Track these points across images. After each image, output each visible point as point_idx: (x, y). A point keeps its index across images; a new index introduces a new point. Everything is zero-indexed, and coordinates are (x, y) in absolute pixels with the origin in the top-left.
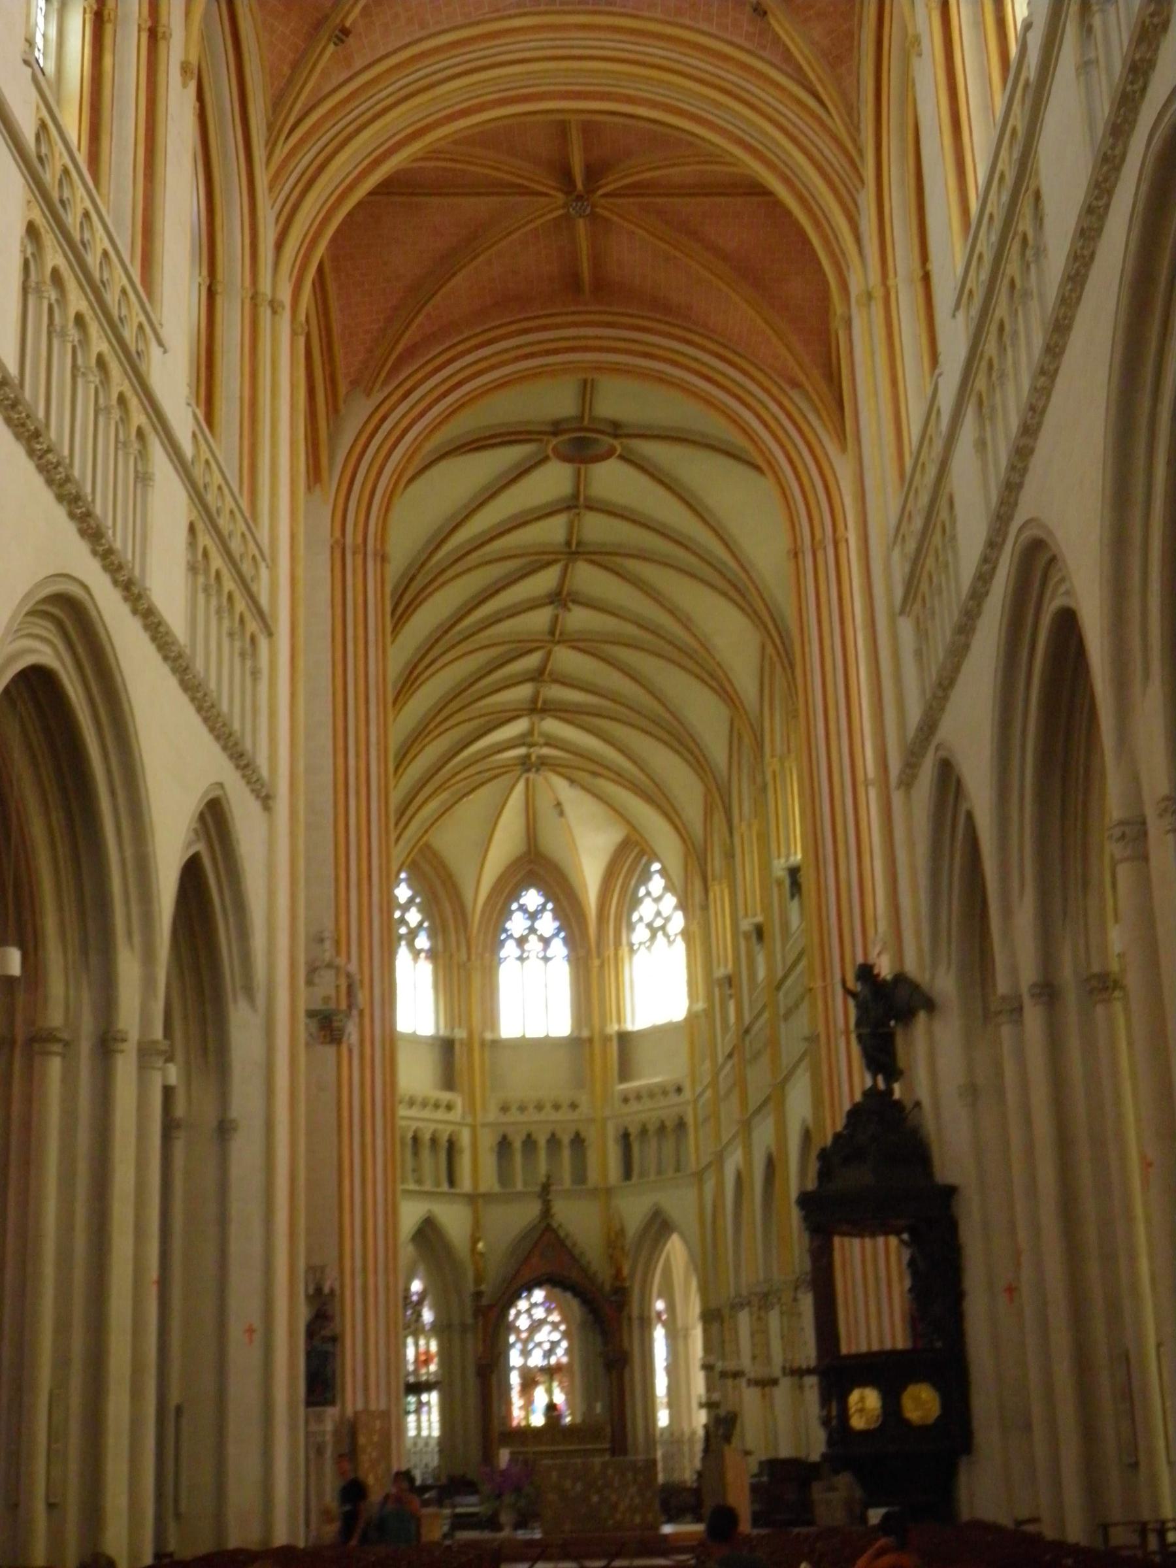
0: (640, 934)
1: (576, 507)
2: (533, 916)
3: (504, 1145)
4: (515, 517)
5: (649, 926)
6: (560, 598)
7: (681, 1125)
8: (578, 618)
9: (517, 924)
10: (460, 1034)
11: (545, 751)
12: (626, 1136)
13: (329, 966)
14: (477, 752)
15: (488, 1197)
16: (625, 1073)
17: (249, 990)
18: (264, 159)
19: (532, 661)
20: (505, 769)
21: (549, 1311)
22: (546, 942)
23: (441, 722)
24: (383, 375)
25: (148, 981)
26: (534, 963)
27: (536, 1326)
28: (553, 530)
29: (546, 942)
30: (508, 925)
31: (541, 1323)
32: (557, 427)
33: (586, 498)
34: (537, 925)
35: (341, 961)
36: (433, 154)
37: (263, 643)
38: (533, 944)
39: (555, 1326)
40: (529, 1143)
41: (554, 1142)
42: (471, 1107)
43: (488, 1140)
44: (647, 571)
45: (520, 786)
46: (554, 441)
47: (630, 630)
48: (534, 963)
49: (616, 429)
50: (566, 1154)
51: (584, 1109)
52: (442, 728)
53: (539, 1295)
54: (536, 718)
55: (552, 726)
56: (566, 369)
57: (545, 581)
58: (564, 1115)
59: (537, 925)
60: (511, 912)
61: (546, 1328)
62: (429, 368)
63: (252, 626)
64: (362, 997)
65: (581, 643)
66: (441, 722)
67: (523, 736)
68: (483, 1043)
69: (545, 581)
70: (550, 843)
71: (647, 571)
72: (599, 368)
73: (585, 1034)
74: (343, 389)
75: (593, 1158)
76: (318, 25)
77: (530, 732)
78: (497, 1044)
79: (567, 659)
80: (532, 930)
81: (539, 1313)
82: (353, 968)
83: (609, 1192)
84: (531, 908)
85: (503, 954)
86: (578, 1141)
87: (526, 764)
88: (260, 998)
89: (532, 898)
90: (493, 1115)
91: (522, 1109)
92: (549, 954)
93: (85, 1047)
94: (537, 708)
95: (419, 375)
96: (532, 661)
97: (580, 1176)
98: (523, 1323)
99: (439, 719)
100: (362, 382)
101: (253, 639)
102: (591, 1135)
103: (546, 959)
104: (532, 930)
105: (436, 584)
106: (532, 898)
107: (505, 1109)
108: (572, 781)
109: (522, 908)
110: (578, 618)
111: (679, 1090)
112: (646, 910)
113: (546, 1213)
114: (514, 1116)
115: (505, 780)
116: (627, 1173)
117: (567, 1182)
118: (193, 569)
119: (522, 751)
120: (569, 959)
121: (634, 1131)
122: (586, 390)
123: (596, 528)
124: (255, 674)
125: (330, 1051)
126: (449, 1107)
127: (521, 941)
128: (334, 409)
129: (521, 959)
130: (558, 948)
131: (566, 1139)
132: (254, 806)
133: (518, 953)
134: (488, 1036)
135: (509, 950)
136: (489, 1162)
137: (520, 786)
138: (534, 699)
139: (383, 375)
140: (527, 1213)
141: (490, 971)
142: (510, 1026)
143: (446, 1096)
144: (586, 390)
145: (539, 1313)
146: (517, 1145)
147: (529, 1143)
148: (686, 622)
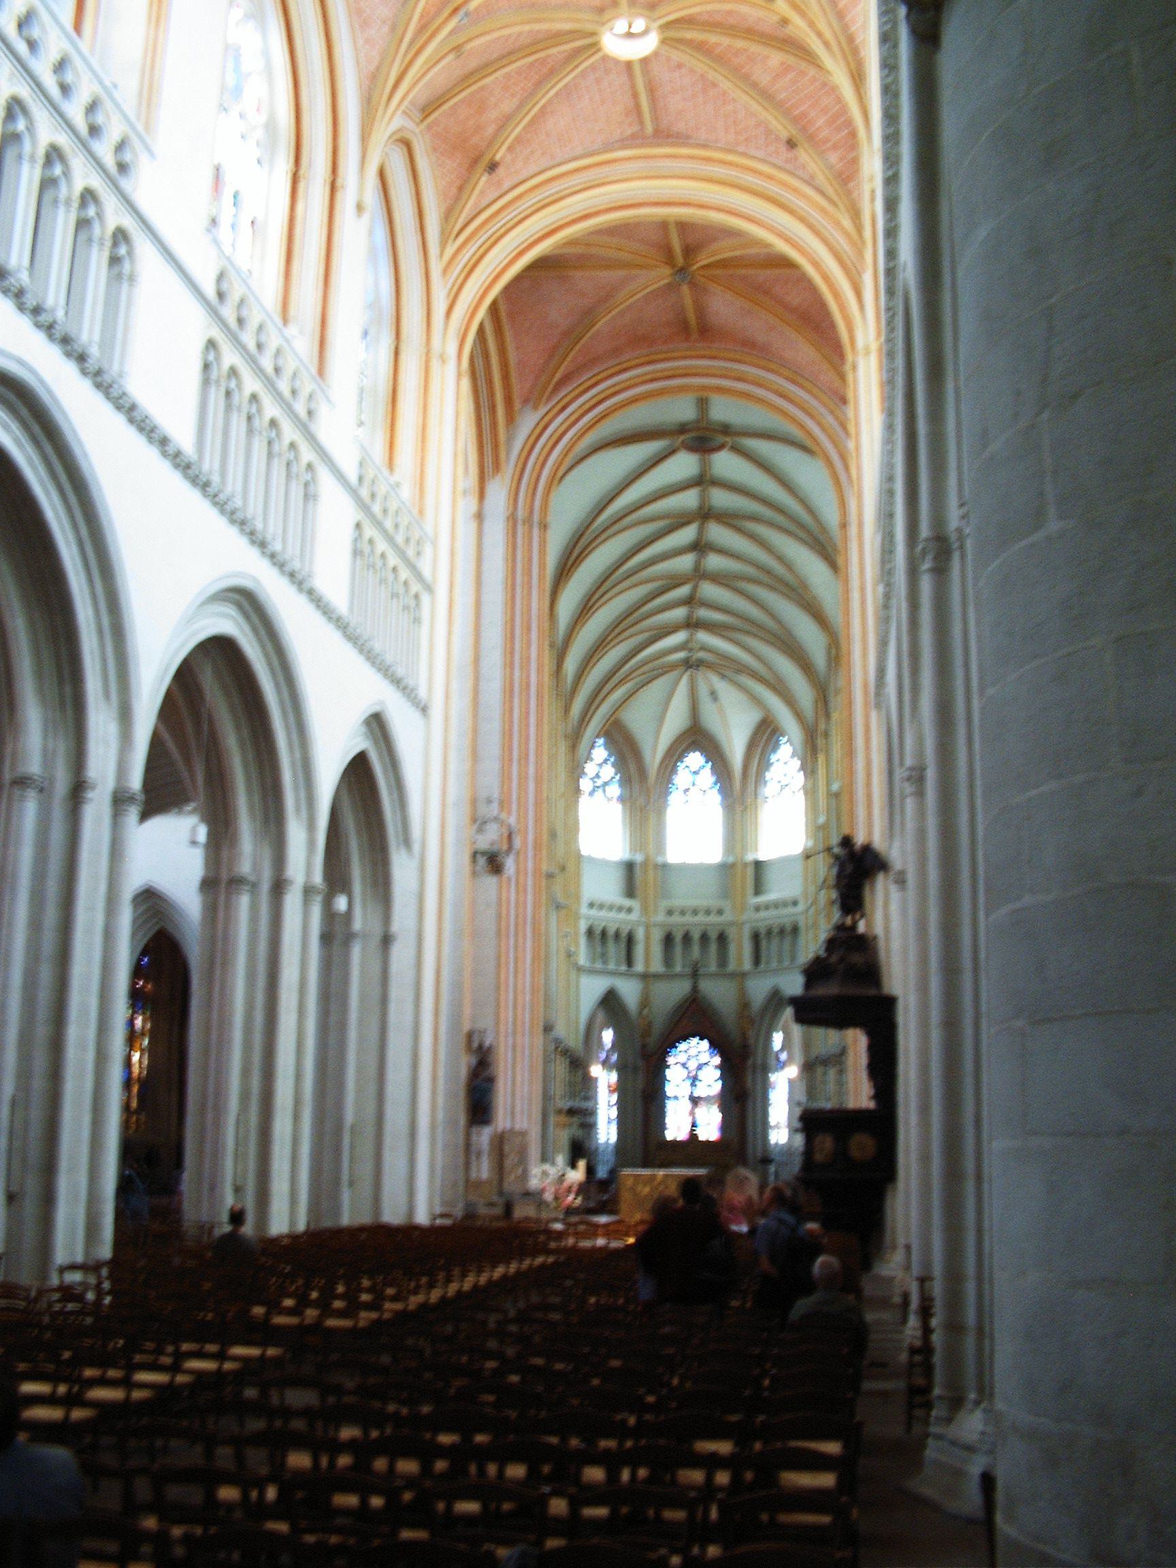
3: (668, 940)
4: (655, 492)
6: (699, 547)
10: (639, 858)
13: (496, 819)
15: (657, 976)
17: (407, 842)
18: (438, 251)
24: (547, 394)
25: (311, 843)
28: (689, 499)
32: (682, 429)
35: (503, 816)
36: (571, 242)
37: (425, 599)
40: (687, 938)
41: (704, 938)
42: (645, 909)
43: (657, 936)
44: (761, 530)
46: (682, 438)
51: (727, 917)
52: (620, 638)
58: (713, 919)
62: (581, 389)
63: (415, 587)
64: (517, 842)
65: (718, 578)
68: (656, 866)
70: (711, 719)
71: (761, 530)
74: (517, 405)
75: (732, 949)
76: (475, 162)
77: (687, 642)
78: (665, 866)
82: (512, 820)
83: (743, 975)
86: (722, 939)
88: (416, 847)
90: (660, 917)
91: (683, 913)
93: (265, 887)
95: (572, 395)
97: (723, 961)
99: (617, 631)
100: (532, 400)
101: (417, 596)
102: (732, 933)
105: (600, 539)
107: (670, 912)
108: (723, 677)
114: (676, 919)
116: (757, 960)
117: (713, 968)
118: (356, 553)
122: (703, 404)
124: (417, 620)
125: (491, 881)
126: (630, 910)
128: (511, 419)
132: (414, 715)
134: (660, 860)
136: (657, 950)
138: (689, 617)
139: (547, 394)
141: (661, 812)
143: (627, 903)
144: (703, 404)
147: (687, 938)
148: (789, 566)
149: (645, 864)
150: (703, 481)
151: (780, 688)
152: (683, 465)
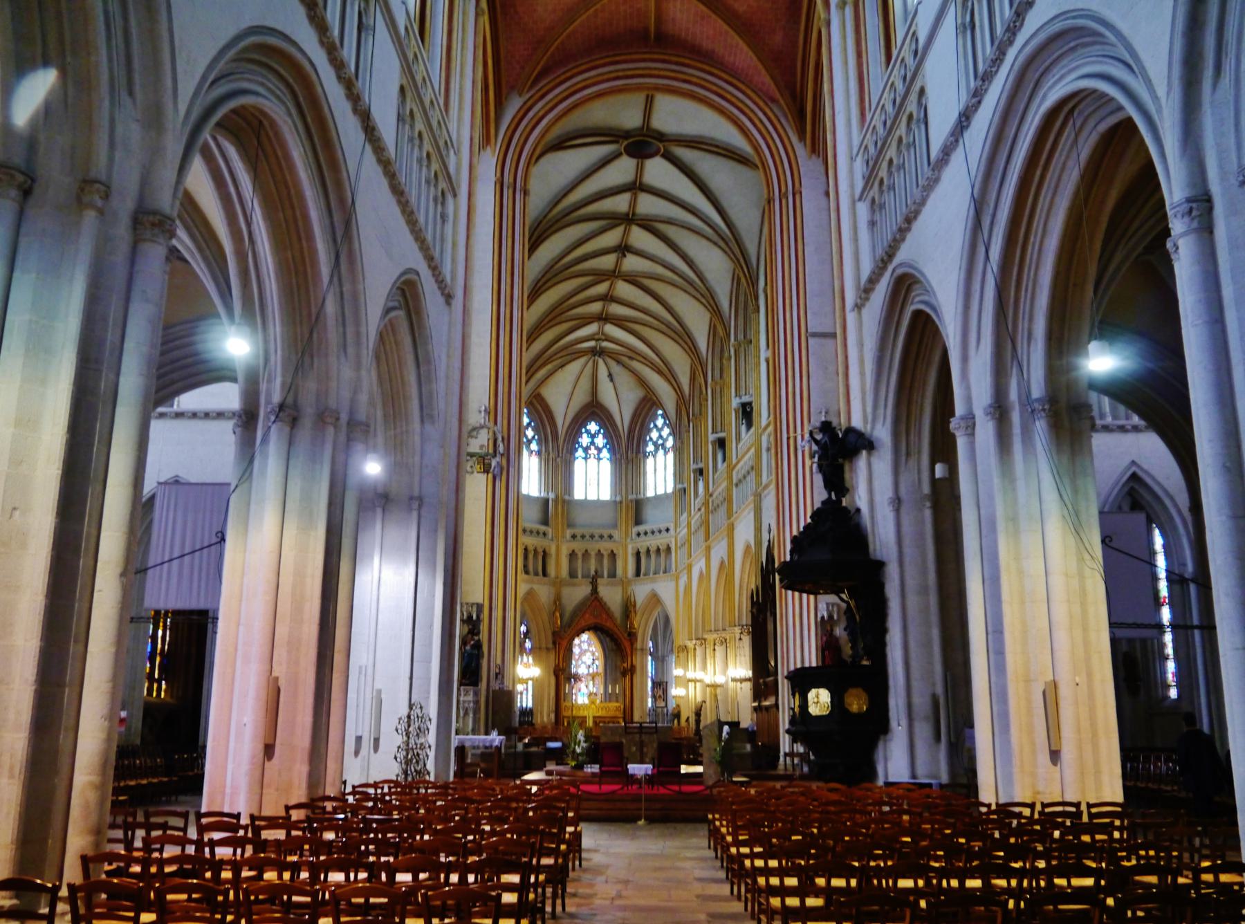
0: (650, 448)
1: (634, 189)
2: (593, 436)
5: (655, 444)
7: (668, 549)
8: (632, 263)
9: (585, 440)
10: (551, 496)
11: (605, 344)
12: (638, 554)
14: (568, 343)
16: (638, 521)
19: (602, 288)
20: (583, 353)
21: (589, 645)
22: (599, 450)
23: (550, 321)
26: (592, 462)
27: (583, 653)
28: (620, 203)
29: (599, 450)
30: (580, 440)
31: (585, 651)
32: (627, 134)
33: (640, 183)
34: (596, 440)
38: (593, 451)
39: (593, 654)
45: (591, 362)
47: (660, 270)
48: (592, 462)
49: (661, 136)
50: (606, 561)
53: (585, 636)
54: (601, 323)
55: (611, 329)
56: (638, 88)
57: (611, 238)
59: (596, 440)
60: (582, 433)
61: (588, 654)
66: (550, 321)
67: (594, 334)
68: (564, 501)
69: (611, 238)
72: (658, 89)
73: (618, 499)
75: (620, 564)
79: (624, 289)
80: (593, 443)
81: (585, 646)
84: (593, 432)
85: (577, 455)
86: (613, 555)
87: (594, 352)
89: (593, 427)
92: (601, 456)
94: (603, 318)
96: (602, 288)
97: (613, 574)
98: (576, 650)
103: (599, 459)
104: (593, 443)
106: (593, 427)
109: (588, 432)
110: (632, 263)
111: (668, 530)
112: (654, 435)
113: (595, 590)
115: (582, 360)
116: (638, 573)
119: (592, 344)
120: (611, 460)
121: (643, 551)
123: (648, 205)
127: (586, 450)
129: (586, 458)
130: (605, 454)
131: (605, 553)
133: (584, 455)
134: (567, 497)
135: (580, 453)
137: (590, 363)
140: (582, 591)
142: (578, 494)
143: (543, 528)
145: (585, 646)
146: (580, 555)
149: (556, 500)
150: (636, 187)
151: (669, 375)
152: (622, 170)
